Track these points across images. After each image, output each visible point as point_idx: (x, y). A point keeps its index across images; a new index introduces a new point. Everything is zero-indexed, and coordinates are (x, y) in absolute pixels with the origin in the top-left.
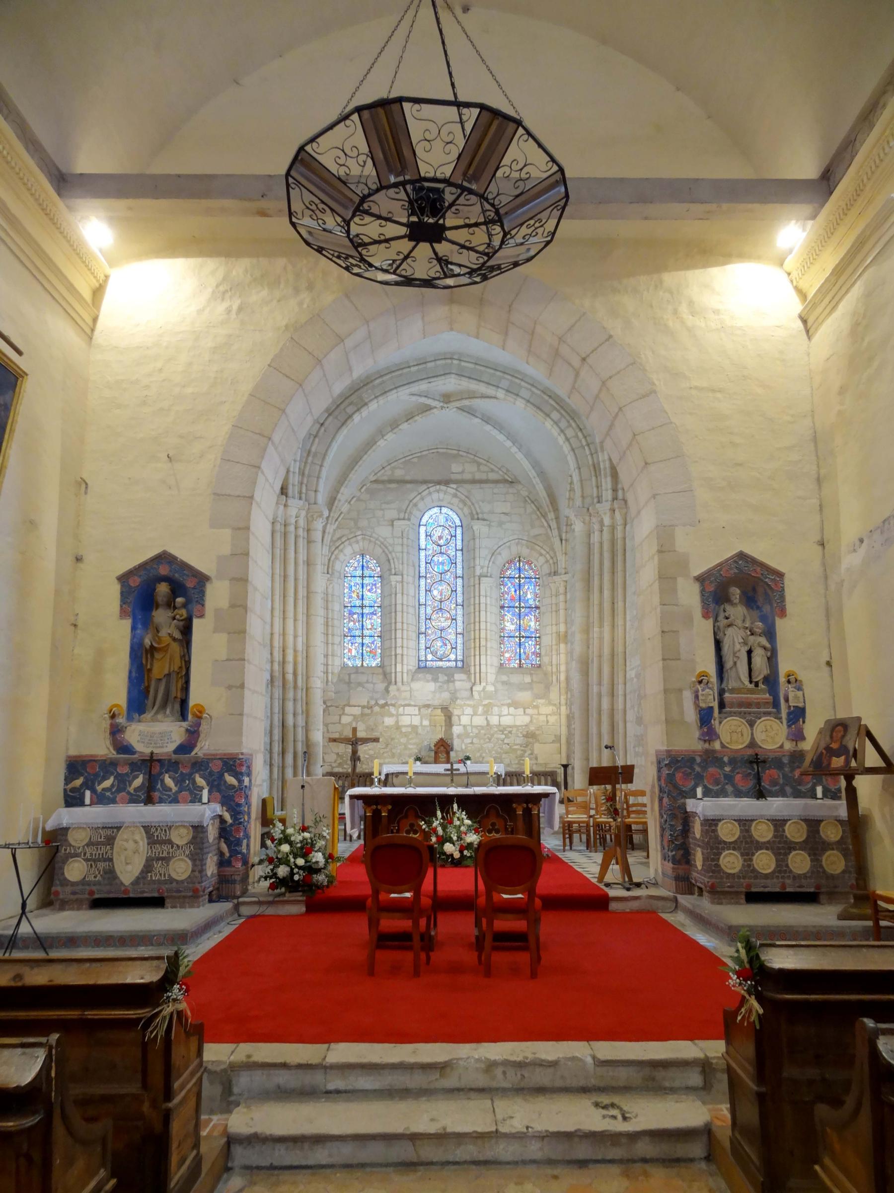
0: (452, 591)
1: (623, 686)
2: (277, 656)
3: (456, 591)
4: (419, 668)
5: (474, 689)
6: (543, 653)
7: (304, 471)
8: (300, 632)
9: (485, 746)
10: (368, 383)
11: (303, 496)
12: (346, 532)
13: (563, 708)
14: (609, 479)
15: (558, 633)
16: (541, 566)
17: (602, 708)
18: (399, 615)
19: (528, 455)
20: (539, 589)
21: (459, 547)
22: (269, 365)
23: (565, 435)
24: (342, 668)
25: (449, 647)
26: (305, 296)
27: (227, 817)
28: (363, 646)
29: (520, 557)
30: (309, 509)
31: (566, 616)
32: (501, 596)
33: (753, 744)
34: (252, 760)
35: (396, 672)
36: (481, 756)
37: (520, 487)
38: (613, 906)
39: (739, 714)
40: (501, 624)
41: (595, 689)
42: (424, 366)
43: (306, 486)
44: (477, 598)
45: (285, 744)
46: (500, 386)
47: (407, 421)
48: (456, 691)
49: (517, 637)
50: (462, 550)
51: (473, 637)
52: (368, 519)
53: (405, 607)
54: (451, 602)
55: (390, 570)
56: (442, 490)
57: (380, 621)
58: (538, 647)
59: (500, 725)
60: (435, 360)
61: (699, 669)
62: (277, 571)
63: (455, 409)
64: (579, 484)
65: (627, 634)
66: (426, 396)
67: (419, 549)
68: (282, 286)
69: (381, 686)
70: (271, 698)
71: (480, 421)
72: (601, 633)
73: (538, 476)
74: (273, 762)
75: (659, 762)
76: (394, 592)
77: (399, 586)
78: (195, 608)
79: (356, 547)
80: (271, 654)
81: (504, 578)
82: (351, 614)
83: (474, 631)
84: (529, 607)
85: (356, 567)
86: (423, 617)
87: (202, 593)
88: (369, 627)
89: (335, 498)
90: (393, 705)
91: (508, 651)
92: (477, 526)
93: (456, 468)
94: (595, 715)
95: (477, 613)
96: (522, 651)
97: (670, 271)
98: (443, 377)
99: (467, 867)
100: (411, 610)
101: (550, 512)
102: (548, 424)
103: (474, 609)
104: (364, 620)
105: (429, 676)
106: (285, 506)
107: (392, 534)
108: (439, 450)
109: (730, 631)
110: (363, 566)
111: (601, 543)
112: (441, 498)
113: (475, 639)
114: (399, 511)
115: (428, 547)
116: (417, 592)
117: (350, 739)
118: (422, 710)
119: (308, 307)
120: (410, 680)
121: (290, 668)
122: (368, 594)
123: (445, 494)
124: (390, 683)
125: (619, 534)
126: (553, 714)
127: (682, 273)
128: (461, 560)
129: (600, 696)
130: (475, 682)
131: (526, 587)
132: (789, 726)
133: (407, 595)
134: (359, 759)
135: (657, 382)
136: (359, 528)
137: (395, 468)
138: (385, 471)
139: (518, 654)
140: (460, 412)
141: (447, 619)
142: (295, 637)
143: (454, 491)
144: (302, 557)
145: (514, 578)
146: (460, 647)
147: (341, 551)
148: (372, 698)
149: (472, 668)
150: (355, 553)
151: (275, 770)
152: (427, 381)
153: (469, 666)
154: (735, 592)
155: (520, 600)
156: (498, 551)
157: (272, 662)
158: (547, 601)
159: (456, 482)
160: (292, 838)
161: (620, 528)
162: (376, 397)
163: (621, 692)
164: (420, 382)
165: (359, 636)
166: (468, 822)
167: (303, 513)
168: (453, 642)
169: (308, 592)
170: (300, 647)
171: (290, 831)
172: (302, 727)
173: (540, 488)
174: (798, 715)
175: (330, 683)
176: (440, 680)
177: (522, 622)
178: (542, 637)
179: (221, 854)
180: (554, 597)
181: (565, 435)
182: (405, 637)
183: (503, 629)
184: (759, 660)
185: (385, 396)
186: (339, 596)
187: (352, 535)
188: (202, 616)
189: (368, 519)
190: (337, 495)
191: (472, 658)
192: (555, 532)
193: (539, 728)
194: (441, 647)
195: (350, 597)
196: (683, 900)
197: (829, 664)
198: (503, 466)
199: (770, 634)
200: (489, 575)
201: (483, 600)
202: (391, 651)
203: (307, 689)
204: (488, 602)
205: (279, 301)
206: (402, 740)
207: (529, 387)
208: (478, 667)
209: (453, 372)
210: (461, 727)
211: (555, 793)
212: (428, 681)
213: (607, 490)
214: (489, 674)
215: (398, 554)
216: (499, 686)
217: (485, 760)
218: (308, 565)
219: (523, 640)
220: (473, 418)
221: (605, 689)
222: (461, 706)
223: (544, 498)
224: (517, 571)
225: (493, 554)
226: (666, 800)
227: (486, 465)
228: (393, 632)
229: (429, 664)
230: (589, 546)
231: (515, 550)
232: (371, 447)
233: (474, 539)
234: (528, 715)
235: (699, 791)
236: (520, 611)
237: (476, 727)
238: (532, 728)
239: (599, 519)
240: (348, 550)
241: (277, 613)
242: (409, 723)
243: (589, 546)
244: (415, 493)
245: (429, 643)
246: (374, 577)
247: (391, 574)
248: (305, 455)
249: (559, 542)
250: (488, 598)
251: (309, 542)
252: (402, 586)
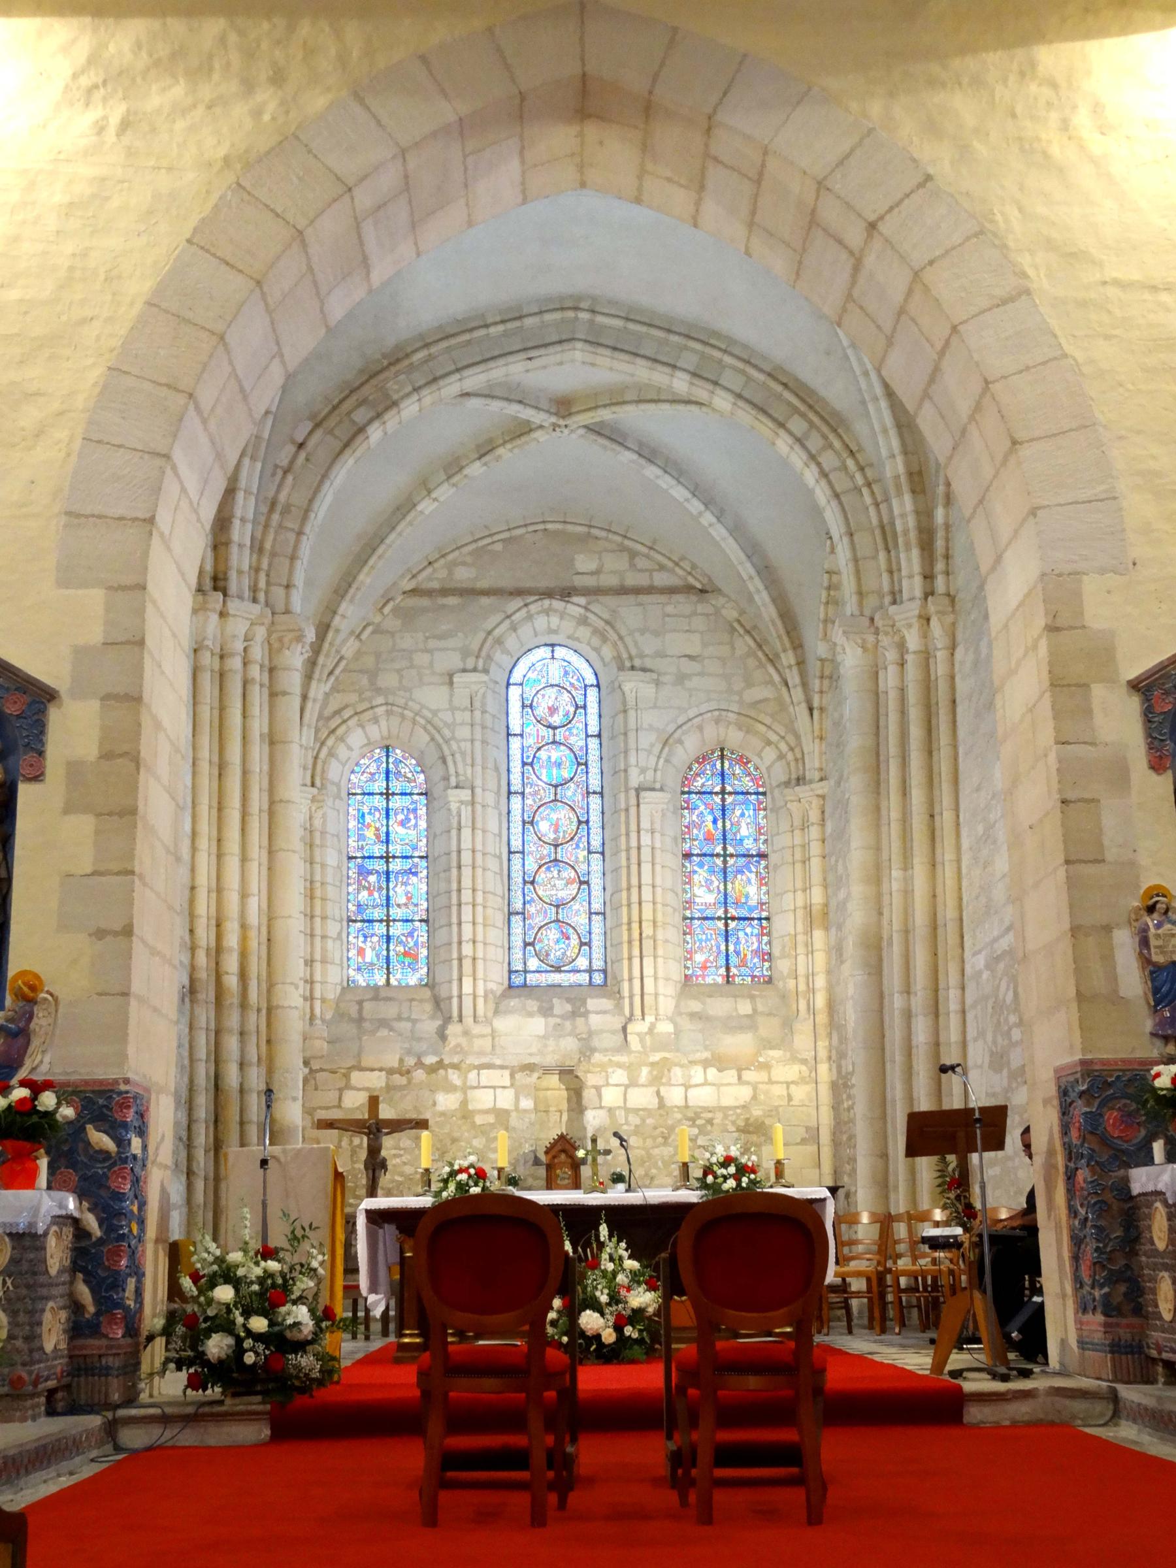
0: (580, 822)
1: (959, 992)
2: (205, 936)
3: (587, 822)
4: (510, 987)
5: (630, 1028)
6: (776, 952)
7: (262, 542)
8: (254, 887)
9: (656, 1151)
10: (398, 361)
11: (261, 596)
12: (353, 698)
13: (823, 1069)
14: (915, 553)
15: (808, 908)
16: (768, 769)
17: (914, 1043)
18: (467, 872)
19: (737, 530)
20: (765, 817)
21: (593, 729)
22: (189, 241)
23: (819, 464)
24: (343, 988)
25: (574, 941)
26: (268, 98)
27: (91, 1222)
28: (388, 942)
29: (722, 750)
30: (273, 623)
31: (824, 872)
32: (683, 833)
34: (148, 1101)
35: (460, 997)
36: (646, 1175)
37: (722, 600)
38: (974, 1414)
40: (685, 891)
41: (897, 1002)
42: (517, 324)
43: (268, 575)
44: (634, 835)
45: (221, 1127)
46: (678, 365)
47: (479, 458)
48: (591, 1034)
49: (719, 918)
50: (599, 736)
51: (625, 920)
52: (398, 671)
53: (479, 856)
54: (578, 846)
55: (446, 778)
56: (556, 611)
57: (424, 888)
58: (765, 939)
59: (687, 1107)
60: (541, 312)
61: (1149, 881)
62: (205, 753)
63: (582, 431)
64: (851, 565)
65: (965, 883)
66: (520, 402)
67: (508, 735)
68: (216, 76)
69: (429, 1026)
70: (191, 1027)
71: (635, 457)
72: (908, 881)
73: (758, 573)
74: (195, 1168)
75: (1064, 1093)
76: (455, 825)
77: (466, 812)
78: (24, 761)
79: (374, 732)
80: (191, 931)
81: (689, 793)
82: (363, 872)
83: (629, 905)
84: (744, 856)
85: (373, 774)
86: (517, 877)
87: (39, 727)
88: (403, 900)
89: (328, 626)
90: (456, 1067)
91: (701, 949)
92: (633, 685)
93: (584, 563)
94: (899, 1058)
95: (634, 868)
96: (731, 948)
97: (1051, 42)
98: (558, 348)
99: (633, 1362)
100: (493, 864)
101: (785, 651)
102: (783, 444)
103: (628, 859)
104: (391, 885)
105: (533, 1005)
106: (222, 614)
107: (451, 701)
108: (549, 526)
110: (388, 772)
111: (902, 690)
112: (554, 626)
113: (629, 923)
114: (465, 653)
115: (527, 730)
116: (505, 825)
117: (365, 1121)
118: (518, 1076)
119: (274, 119)
120: (490, 1014)
121: (231, 964)
122: (397, 831)
123: (562, 618)
124: (448, 1020)
125: (940, 669)
126: (802, 1081)
127: (1078, 45)
128: (597, 758)
129: (908, 1015)
130: (632, 1014)
131: (738, 813)
133: (484, 831)
134: (383, 1165)
135: (1031, 272)
136: (378, 691)
137: (454, 563)
138: (435, 571)
139: (723, 955)
140: (594, 437)
141: (569, 882)
142: (244, 896)
143: (582, 611)
144: (259, 725)
145: (711, 793)
146: (597, 941)
147: (342, 739)
148: (409, 1052)
149: (626, 985)
150: (370, 745)
151: (200, 1185)
152: (523, 356)
153: (619, 982)
155: (725, 839)
156: (676, 735)
157: (193, 949)
158: (784, 840)
159: (586, 592)
160: (241, 1272)
161: (941, 655)
162: (416, 390)
163: (954, 1006)
164: (510, 359)
165: (381, 921)
166: (632, 1264)
167: (261, 633)
168: (583, 930)
169: (272, 803)
170: (253, 918)
171: (235, 1257)
172: (259, 1093)
173: (763, 598)
175: (318, 1022)
176: (557, 1010)
177: (729, 886)
178: (774, 919)
179: (76, 1307)
180: (797, 832)
181: (819, 464)
182: (480, 919)
183: (689, 903)
185: (434, 387)
186: (337, 836)
187: (366, 705)
188: (37, 777)
189: (398, 671)
190: (333, 618)
191: (626, 962)
192: (798, 694)
193: (774, 1112)
194: (558, 941)
195: (361, 837)
196: (1131, 1394)
198: (683, 558)
200: (658, 786)
201: (646, 839)
202: (450, 951)
203: (270, 1010)
204: (658, 845)
205: (209, 107)
206: (475, 1143)
207: (740, 365)
208: (637, 983)
209: (577, 336)
210: (602, 1114)
211: (824, 1200)
212: (530, 1015)
213: (911, 577)
214: (661, 998)
215: (463, 744)
216: (685, 1023)
217: (656, 1182)
218: (272, 743)
219: (732, 924)
220: (618, 448)
221: (919, 1000)
222: (603, 1067)
223: (773, 621)
224: (719, 779)
225: (665, 743)
226: (1083, 1175)
227: (647, 557)
228: (454, 909)
229: (532, 979)
230: (876, 696)
231: (712, 734)
232: (404, 516)
233: (625, 711)
234: (748, 1083)
235: (1158, 1148)
236: (725, 862)
237: (636, 1111)
238: (757, 1112)
239: (896, 638)
240: (356, 738)
241: (203, 843)
242: (490, 1105)
243: (876, 696)
244: (503, 616)
245: (532, 933)
246: (411, 794)
247: (447, 788)
248: (264, 509)
249: (806, 712)
250: (657, 835)
251: (273, 695)
252: (473, 812)
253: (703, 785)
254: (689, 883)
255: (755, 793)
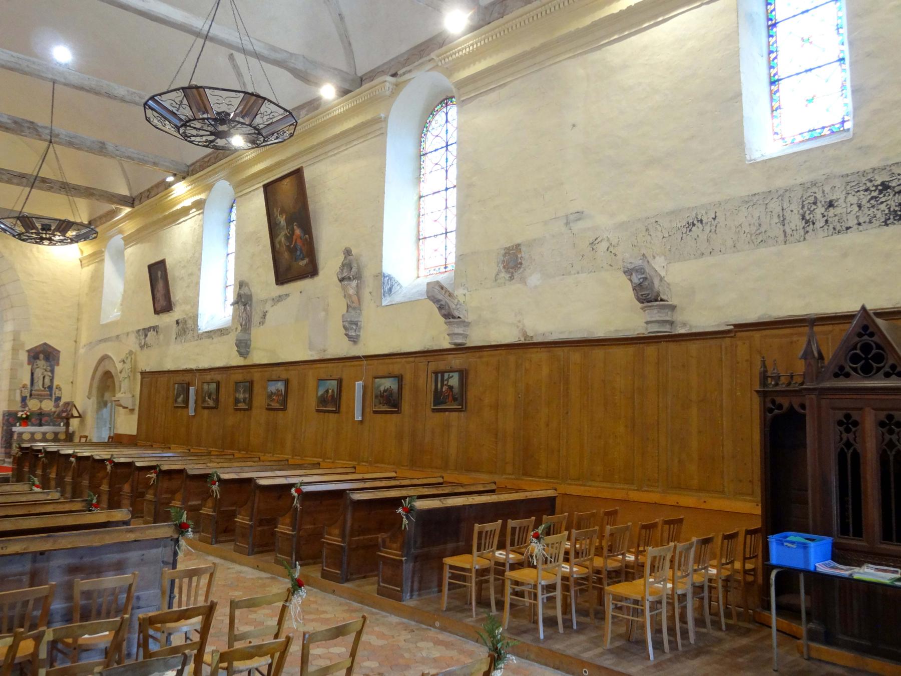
33: (40, 409)
39: (38, 399)
61: (25, 382)
75: (4, 414)
109: (38, 370)
132: (55, 402)
154: (41, 356)
174: (58, 399)
184: (47, 380)
196: (6, 460)
197: (72, 383)
199: (52, 371)
235: (18, 424)
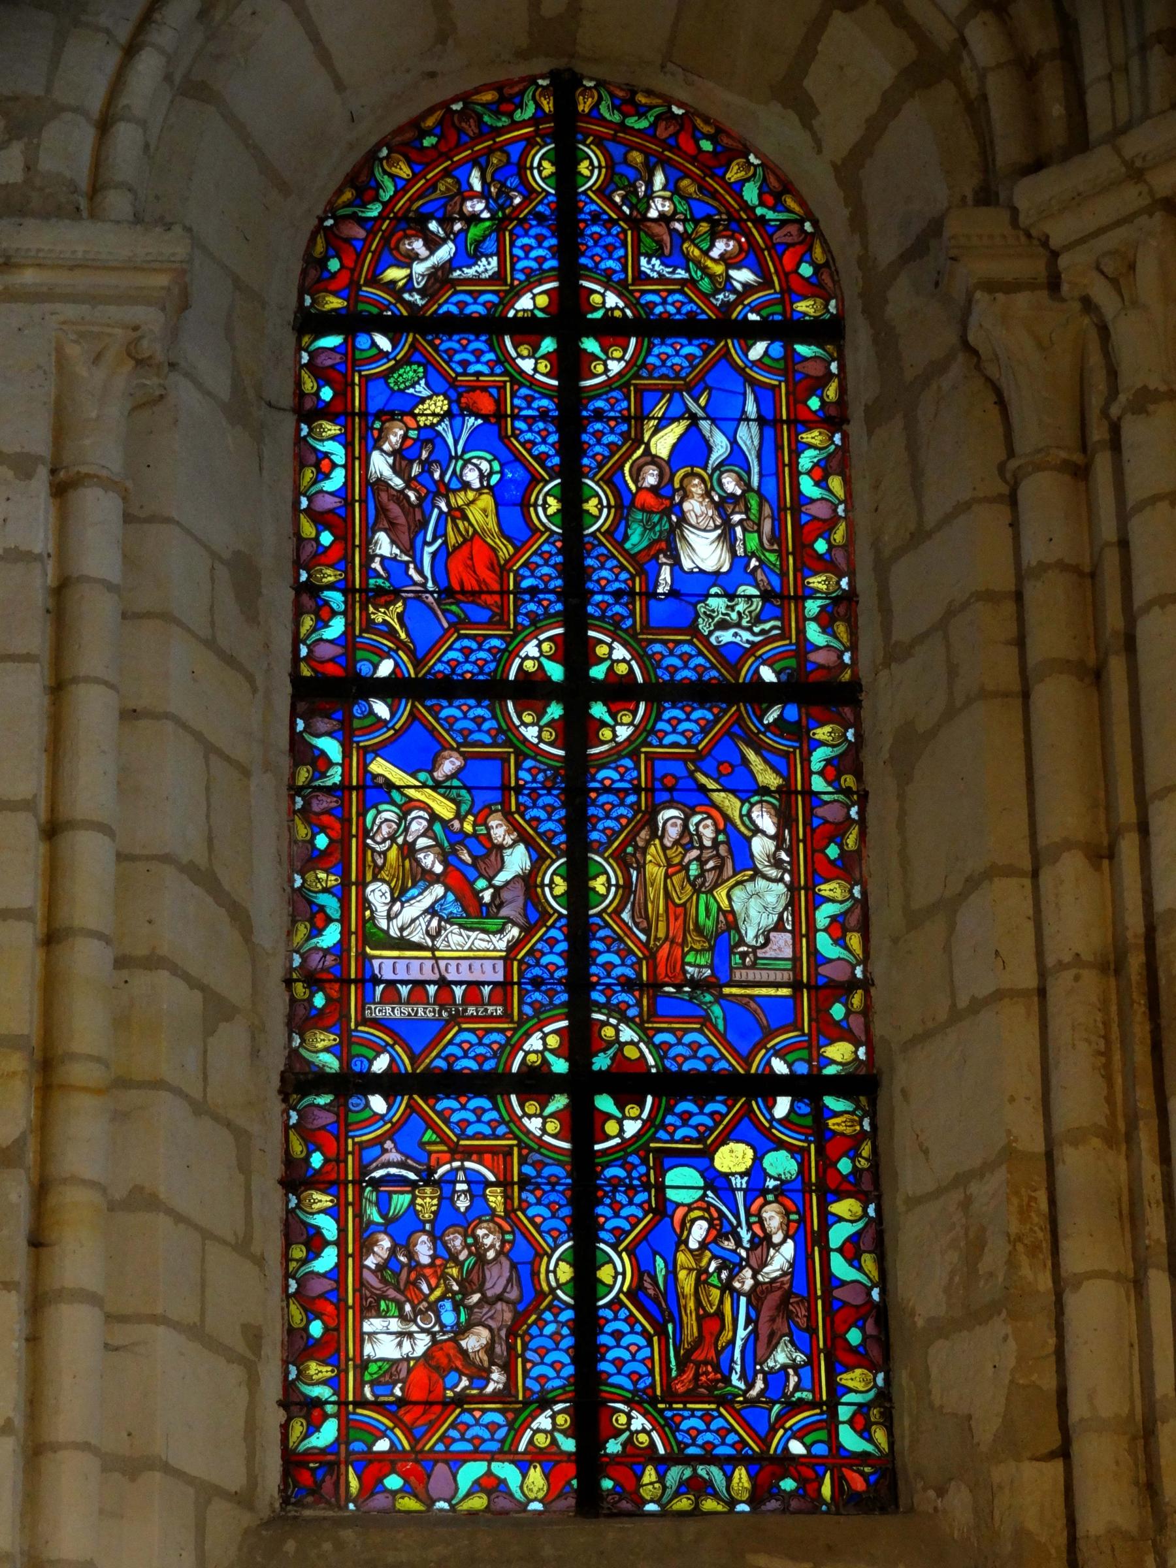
253: (440, 278)
254: (336, 858)
255: (762, 331)
